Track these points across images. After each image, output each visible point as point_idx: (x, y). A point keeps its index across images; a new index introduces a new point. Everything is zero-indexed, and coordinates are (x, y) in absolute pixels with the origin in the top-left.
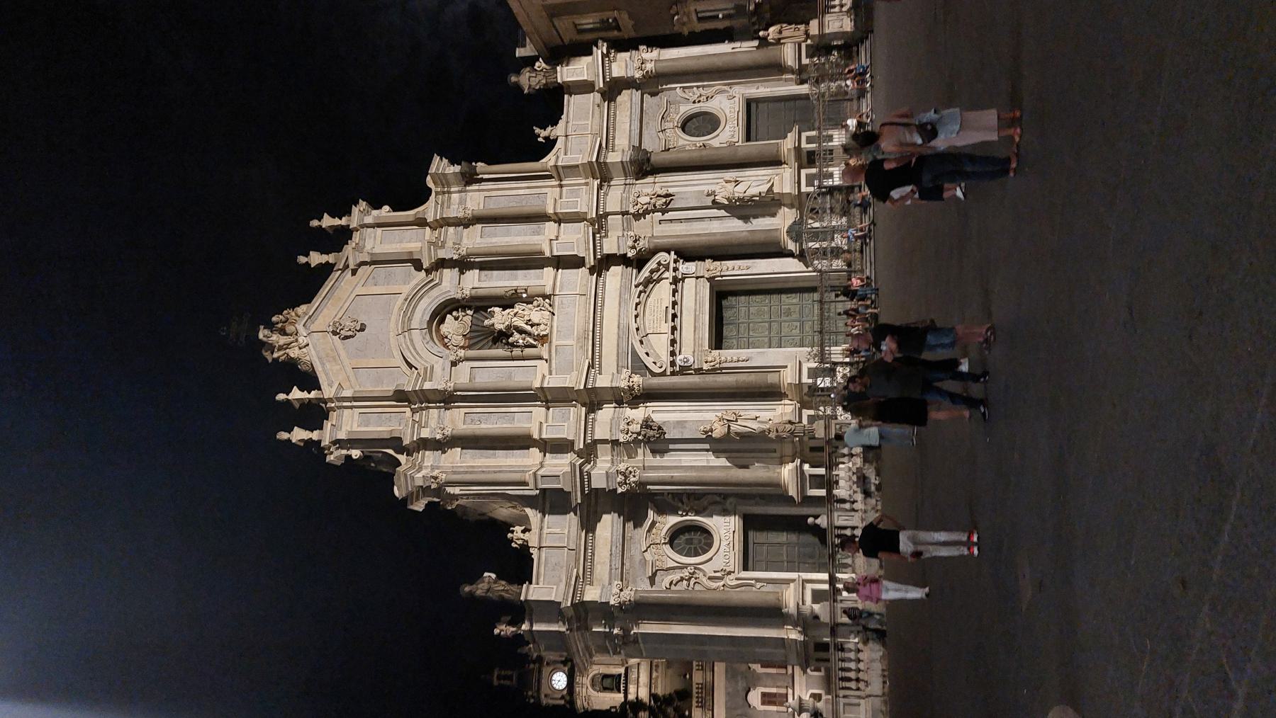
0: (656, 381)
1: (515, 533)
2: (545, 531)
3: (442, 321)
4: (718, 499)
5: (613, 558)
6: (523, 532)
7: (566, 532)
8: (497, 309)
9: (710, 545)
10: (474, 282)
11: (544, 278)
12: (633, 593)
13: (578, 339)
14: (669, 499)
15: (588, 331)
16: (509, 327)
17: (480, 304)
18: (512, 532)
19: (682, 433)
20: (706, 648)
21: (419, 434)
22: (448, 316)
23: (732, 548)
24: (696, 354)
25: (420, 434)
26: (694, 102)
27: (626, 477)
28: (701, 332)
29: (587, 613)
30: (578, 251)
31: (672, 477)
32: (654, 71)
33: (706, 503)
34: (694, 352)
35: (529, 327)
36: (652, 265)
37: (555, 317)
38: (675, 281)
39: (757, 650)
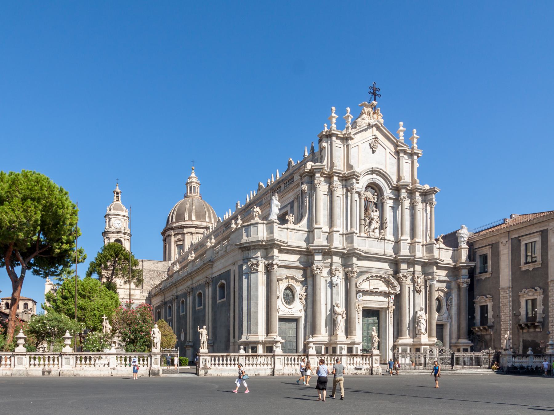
0: (353, 283)
1: (292, 217)
3: (372, 188)
5: (284, 261)
6: (293, 222)
7: (294, 241)
8: (377, 214)
9: (286, 303)
10: (389, 204)
11: (389, 234)
12: (276, 270)
13: (369, 250)
16: (372, 219)
17: (380, 205)
18: (293, 216)
19: (335, 294)
22: (374, 191)
27: (320, 269)
29: (265, 249)
31: (320, 289)
37: (377, 240)
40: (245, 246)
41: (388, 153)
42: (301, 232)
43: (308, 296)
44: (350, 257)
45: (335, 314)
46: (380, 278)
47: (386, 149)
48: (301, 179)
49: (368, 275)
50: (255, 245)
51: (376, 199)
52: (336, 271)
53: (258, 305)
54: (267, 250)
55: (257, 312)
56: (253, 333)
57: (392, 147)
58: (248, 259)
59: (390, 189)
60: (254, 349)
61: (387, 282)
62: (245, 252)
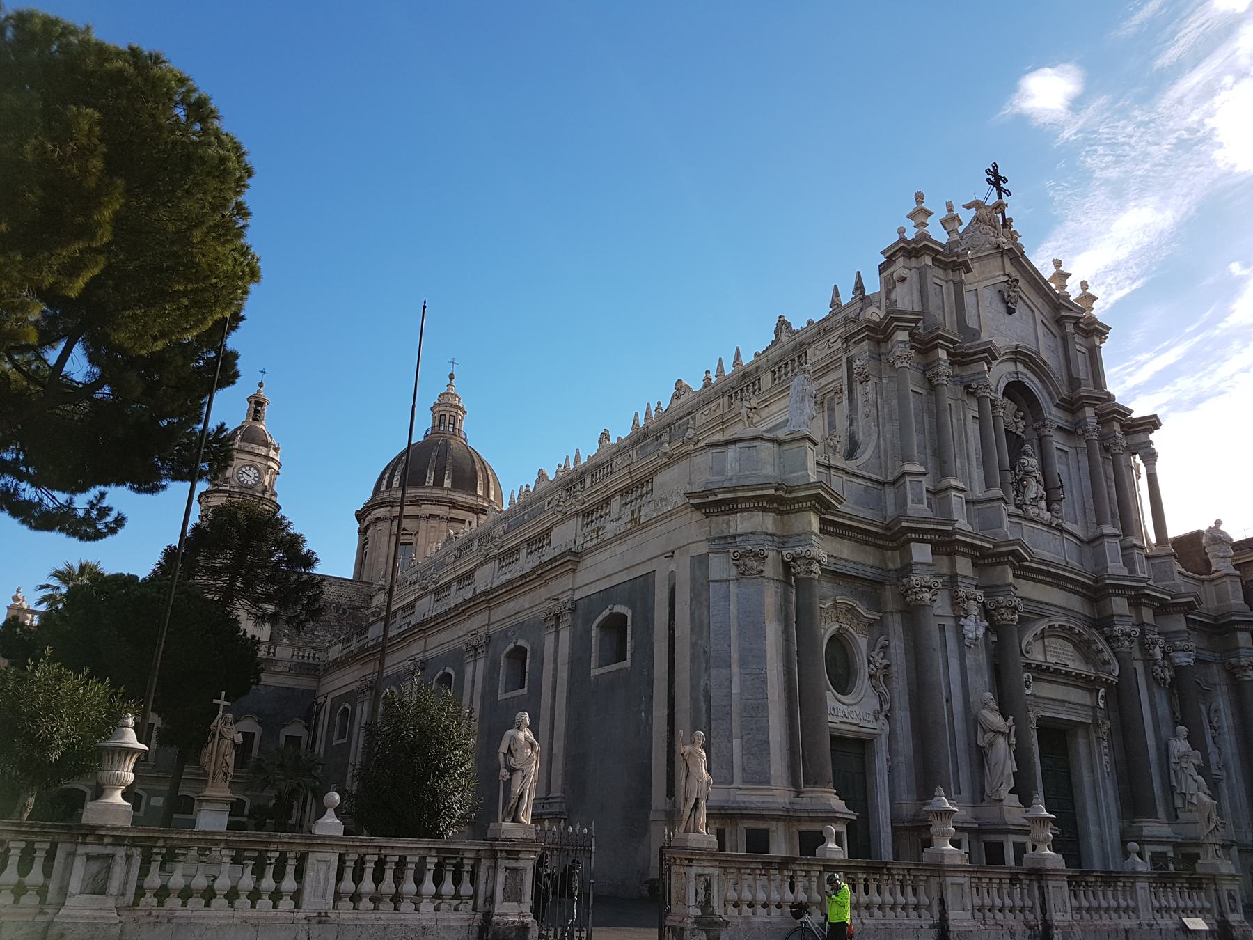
2: (846, 477)
4: (886, 707)
14: (881, 640)
15: (1049, 566)
20: (735, 669)
21: (943, 347)
23: (842, 720)
24: (1033, 698)
25: (941, 348)
26: (1210, 722)
28: (1050, 707)
30: (1113, 567)
32: (1246, 679)
33: (881, 690)
34: (1034, 695)
35: (1034, 496)
36: (1107, 655)
38: (1097, 678)
39: (737, 743)
40: (720, 500)
41: (1038, 321)
42: (860, 481)
43: (894, 668)
44: (997, 564)
45: (985, 732)
46: (1065, 633)
47: (1033, 311)
48: (847, 350)
49: (1042, 625)
50: (754, 497)
51: (1021, 428)
52: (969, 600)
53: (765, 681)
54: (786, 516)
55: (765, 707)
56: (752, 782)
57: (1046, 310)
58: (726, 537)
59: (1057, 406)
60: (758, 842)
61: (1083, 647)
62: (714, 518)
